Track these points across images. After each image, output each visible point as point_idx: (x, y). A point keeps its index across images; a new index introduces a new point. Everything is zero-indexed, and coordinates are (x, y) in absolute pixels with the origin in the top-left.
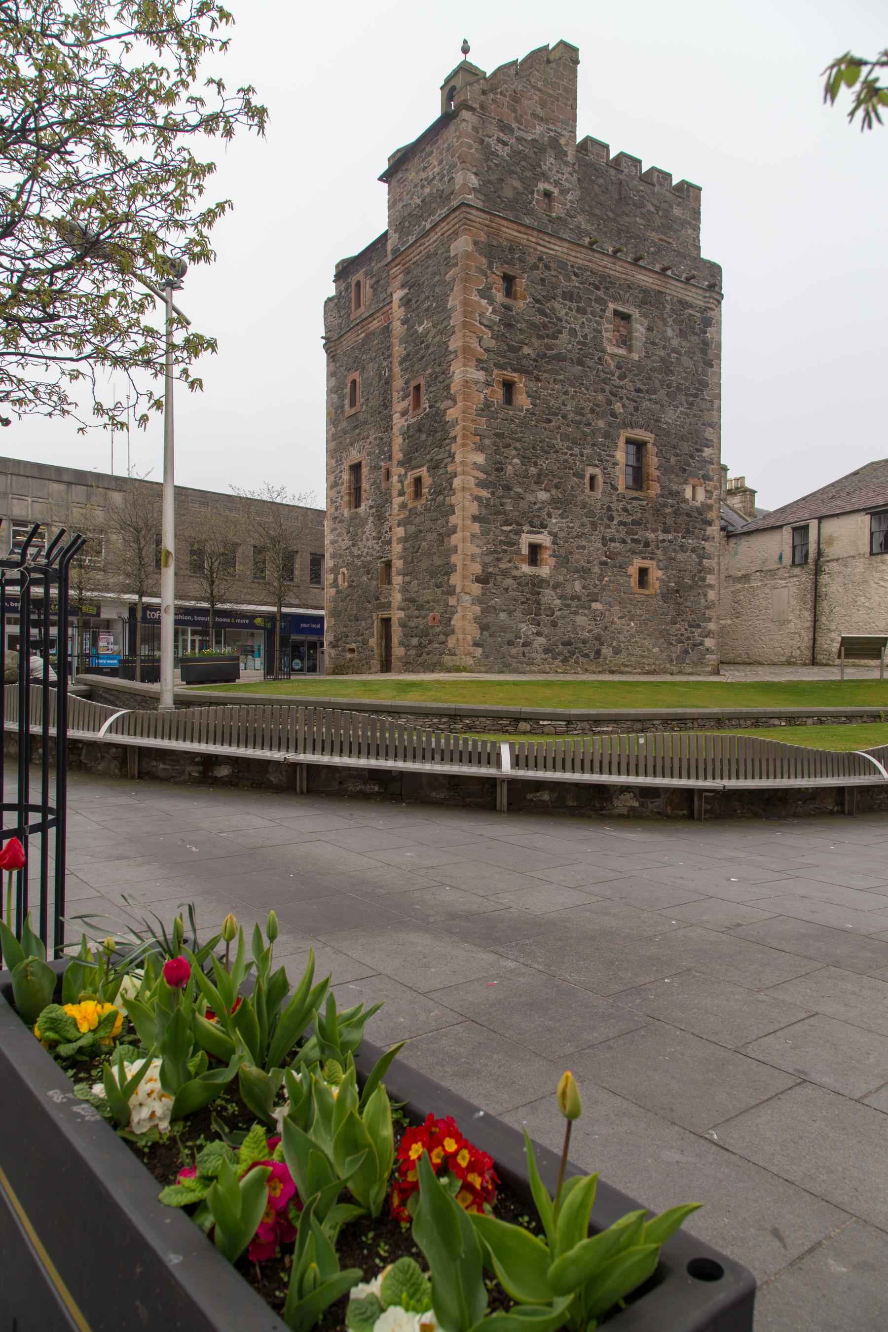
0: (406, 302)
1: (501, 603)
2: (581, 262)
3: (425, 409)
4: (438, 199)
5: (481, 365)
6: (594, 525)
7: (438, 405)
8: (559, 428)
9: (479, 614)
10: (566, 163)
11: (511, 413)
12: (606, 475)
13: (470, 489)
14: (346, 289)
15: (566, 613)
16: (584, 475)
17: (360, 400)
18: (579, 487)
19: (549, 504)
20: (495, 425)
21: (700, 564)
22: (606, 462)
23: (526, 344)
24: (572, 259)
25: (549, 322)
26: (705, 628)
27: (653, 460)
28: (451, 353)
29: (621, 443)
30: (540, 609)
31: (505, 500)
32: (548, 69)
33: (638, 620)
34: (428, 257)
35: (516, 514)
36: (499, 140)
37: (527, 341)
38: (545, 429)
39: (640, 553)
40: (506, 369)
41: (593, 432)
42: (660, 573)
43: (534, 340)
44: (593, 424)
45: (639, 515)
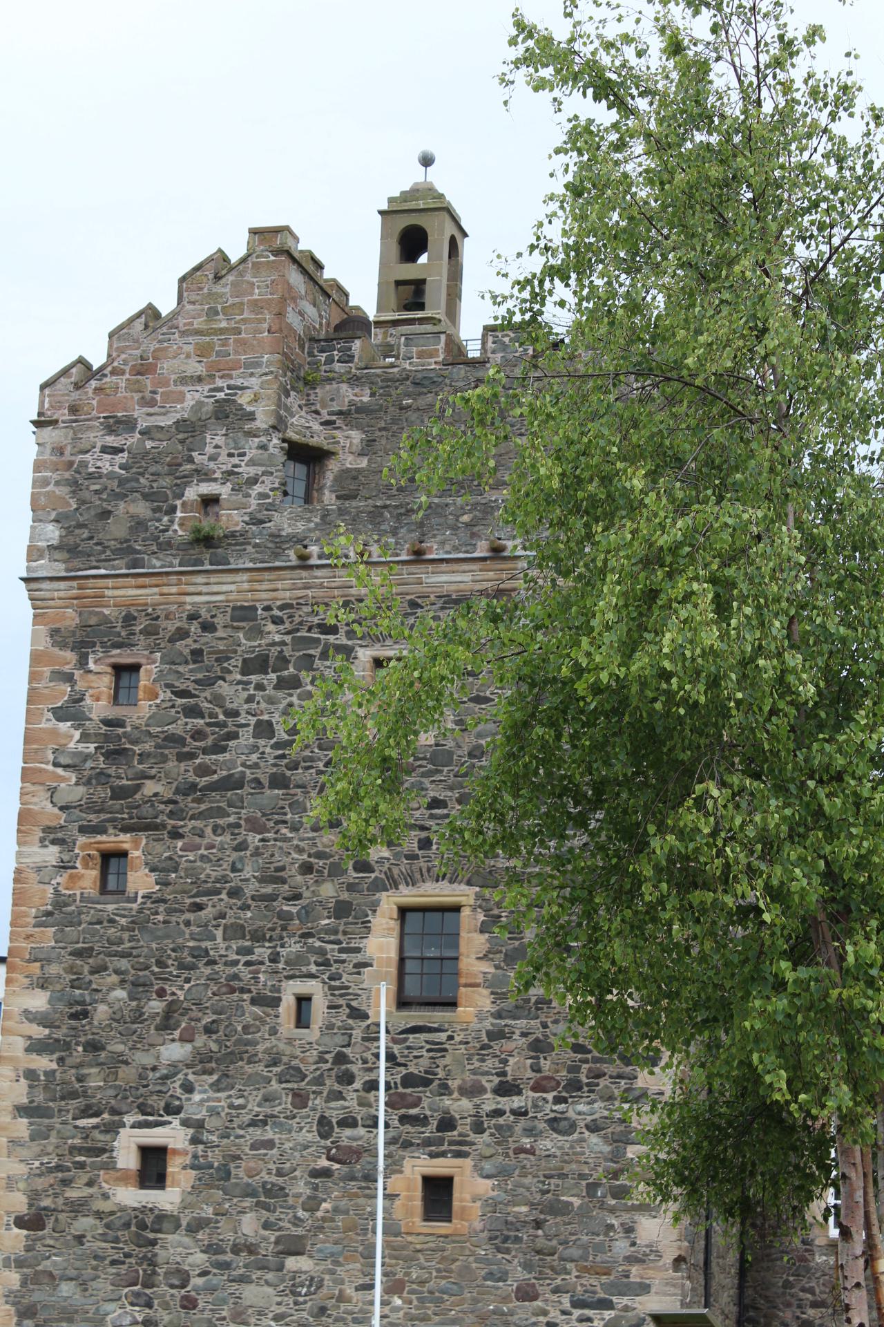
1: (65, 1265)
2: (288, 594)
5: (52, 836)
6: (300, 1099)
8: (222, 916)
9: (17, 1286)
10: (252, 434)
11: (110, 907)
12: (336, 988)
13: (11, 1059)
15: (218, 1278)
16: (279, 999)
18: (264, 1023)
19: (188, 1066)
20: (74, 936)
21: (616, 1156)
22: (338, 965)
23: (153, 777)
24: (264, 595)
25: (208, 724)
26: (626, 1308)
27: (472, 943)
30: (154, 1273)
31: (85, 1071)
32: (218, 289)
33: (412, 1292)
35: (112, 1092)
36: (105, 450)
37: (153, 772)
38: (188, 923)
39: (427, 1143)
40: (103, 831)
41: (307, 912)
42: (485, 1187)
43: (171, 764)
44: (306, 894)
45: (425, 1063)
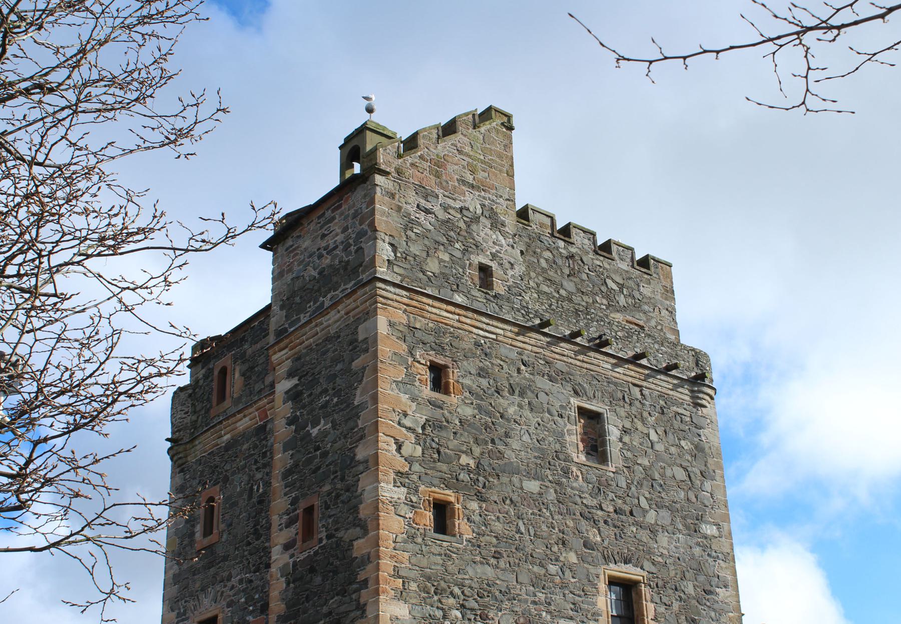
0: (294, 396)
3: (321, 540)
4: (342, 271)
7: (339, 535)
14: (206, 377)
17: (219, 526)
28: (359, 462)
29: (603, 586)
34: (326, 340)
44: (562, 559)
